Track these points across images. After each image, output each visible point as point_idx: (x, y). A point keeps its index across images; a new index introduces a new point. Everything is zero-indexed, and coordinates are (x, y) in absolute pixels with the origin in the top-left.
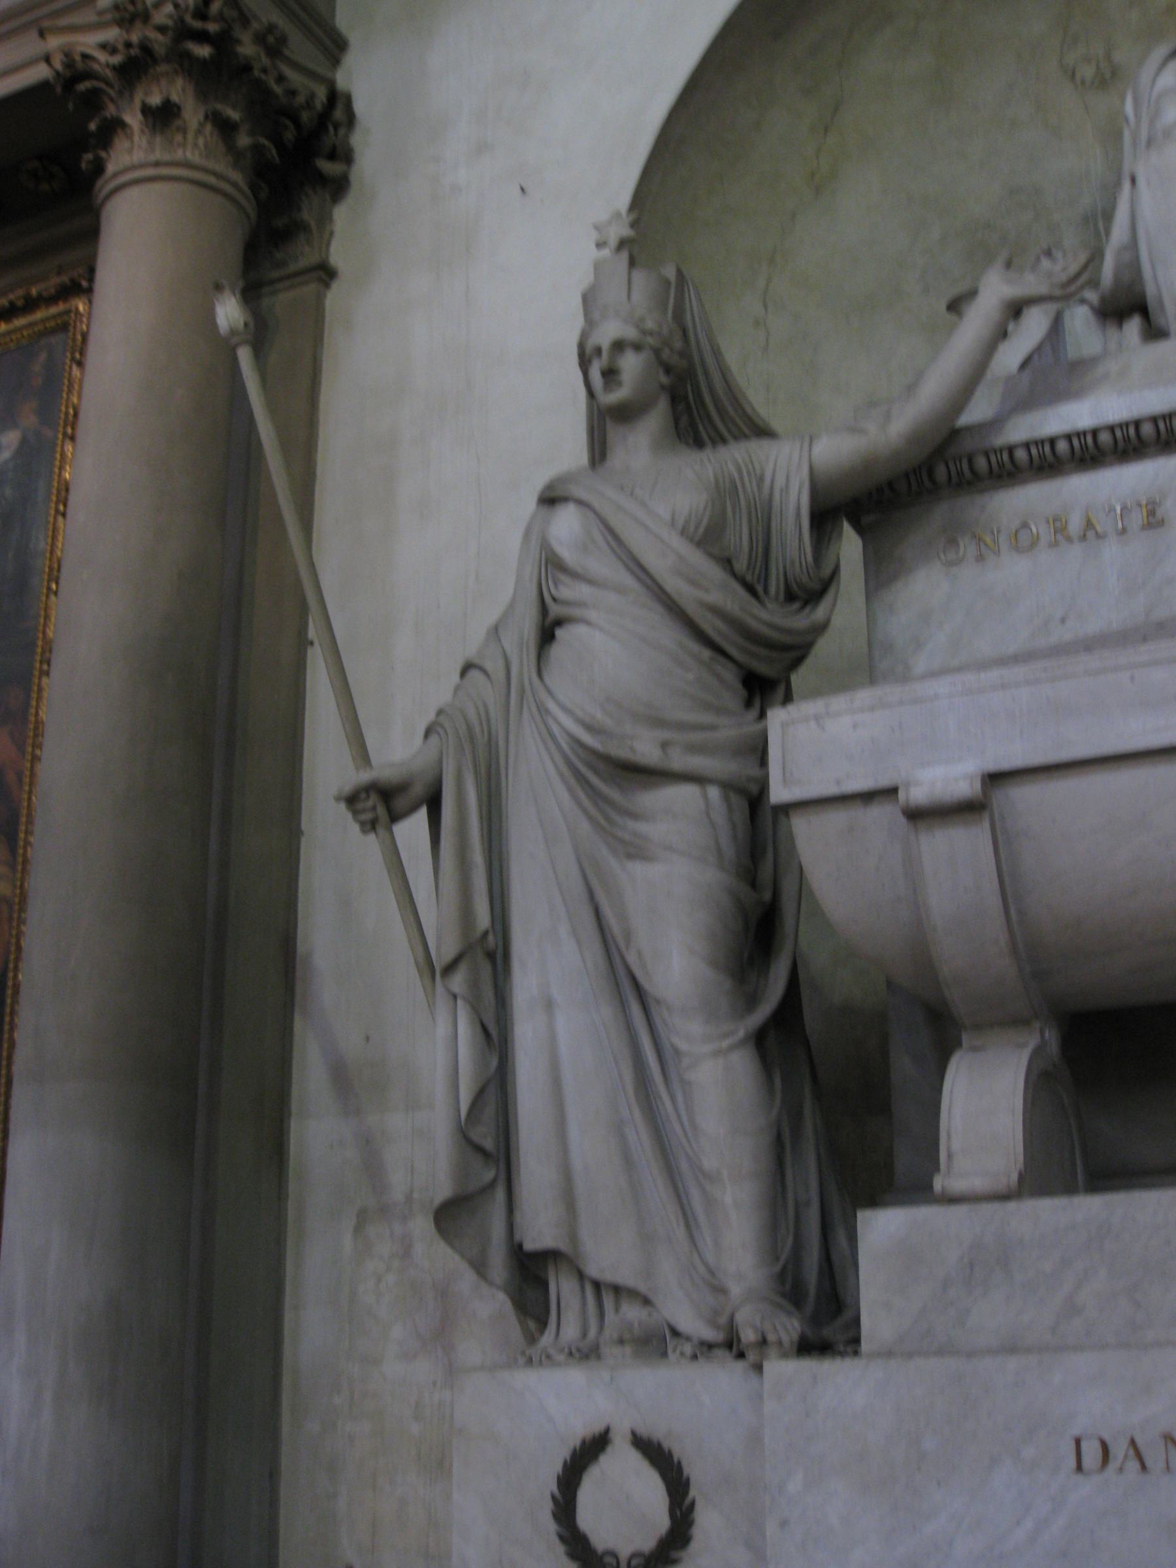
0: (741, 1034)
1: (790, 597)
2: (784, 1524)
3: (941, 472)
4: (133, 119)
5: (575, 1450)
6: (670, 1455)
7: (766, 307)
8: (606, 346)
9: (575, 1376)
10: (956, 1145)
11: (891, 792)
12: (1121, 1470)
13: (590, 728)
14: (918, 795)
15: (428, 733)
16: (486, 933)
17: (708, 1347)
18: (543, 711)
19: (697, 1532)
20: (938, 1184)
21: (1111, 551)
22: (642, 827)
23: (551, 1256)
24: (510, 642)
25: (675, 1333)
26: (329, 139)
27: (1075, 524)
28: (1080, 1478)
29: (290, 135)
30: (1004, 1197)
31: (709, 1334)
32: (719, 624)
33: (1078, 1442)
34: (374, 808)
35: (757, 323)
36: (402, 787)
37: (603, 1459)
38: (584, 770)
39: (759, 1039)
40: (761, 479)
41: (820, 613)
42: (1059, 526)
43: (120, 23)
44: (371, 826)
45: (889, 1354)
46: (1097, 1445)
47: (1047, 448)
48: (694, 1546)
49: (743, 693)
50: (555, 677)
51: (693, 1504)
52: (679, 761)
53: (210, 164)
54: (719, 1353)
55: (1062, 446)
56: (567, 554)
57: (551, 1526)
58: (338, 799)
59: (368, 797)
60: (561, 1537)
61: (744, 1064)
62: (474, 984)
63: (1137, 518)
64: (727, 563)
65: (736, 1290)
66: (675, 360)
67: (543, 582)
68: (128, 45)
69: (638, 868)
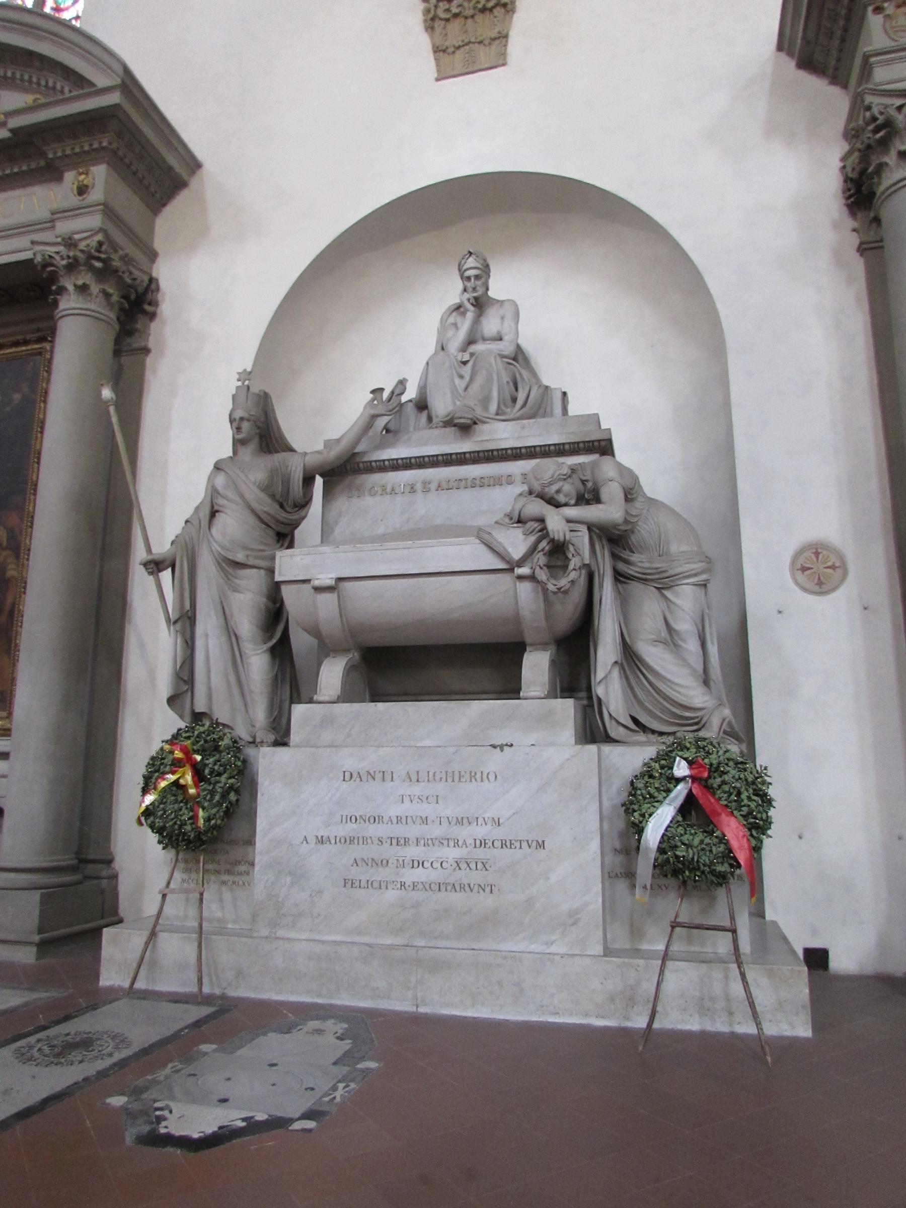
0: (265, 649)
1: (295, 506)
2: (263, 795)
3: (348, 468)
4: (71, 288)
12: (355, 781)
13: (223, 548)
14: (317, 583)
16: (188, 611)
17: (250, 743)
18: (209, 541)
20: (315, 697)
21: (399, 499)
22: (237, 581)
23: (203, 714)
24: (201, 515)
26: (149, 296)
27: (389, 489)
28: (344, 782)
29: (133, 296)
31: (251, 740)
32: (269, 518)
33: (344, 772)
34: (152, 568)
38: (220, 561)
39: (273, 651)
40: (287, 467)
41: (303, 513)
43: (65, 246)
44: (151, 573)
45: (297, 746)
46: (349, 774)
49: (276, 538)
50: (214, 531)
52: (251, 562)
53: (99, 309)
55: (387, 463)
56: (220, 489)
58: (140, 564)
62: (184, 628)
63: (408, 488)
64: (273, 496)
65: (258, 725)
66: (261, 425)
68: (69, 257)
69: (237, 595)
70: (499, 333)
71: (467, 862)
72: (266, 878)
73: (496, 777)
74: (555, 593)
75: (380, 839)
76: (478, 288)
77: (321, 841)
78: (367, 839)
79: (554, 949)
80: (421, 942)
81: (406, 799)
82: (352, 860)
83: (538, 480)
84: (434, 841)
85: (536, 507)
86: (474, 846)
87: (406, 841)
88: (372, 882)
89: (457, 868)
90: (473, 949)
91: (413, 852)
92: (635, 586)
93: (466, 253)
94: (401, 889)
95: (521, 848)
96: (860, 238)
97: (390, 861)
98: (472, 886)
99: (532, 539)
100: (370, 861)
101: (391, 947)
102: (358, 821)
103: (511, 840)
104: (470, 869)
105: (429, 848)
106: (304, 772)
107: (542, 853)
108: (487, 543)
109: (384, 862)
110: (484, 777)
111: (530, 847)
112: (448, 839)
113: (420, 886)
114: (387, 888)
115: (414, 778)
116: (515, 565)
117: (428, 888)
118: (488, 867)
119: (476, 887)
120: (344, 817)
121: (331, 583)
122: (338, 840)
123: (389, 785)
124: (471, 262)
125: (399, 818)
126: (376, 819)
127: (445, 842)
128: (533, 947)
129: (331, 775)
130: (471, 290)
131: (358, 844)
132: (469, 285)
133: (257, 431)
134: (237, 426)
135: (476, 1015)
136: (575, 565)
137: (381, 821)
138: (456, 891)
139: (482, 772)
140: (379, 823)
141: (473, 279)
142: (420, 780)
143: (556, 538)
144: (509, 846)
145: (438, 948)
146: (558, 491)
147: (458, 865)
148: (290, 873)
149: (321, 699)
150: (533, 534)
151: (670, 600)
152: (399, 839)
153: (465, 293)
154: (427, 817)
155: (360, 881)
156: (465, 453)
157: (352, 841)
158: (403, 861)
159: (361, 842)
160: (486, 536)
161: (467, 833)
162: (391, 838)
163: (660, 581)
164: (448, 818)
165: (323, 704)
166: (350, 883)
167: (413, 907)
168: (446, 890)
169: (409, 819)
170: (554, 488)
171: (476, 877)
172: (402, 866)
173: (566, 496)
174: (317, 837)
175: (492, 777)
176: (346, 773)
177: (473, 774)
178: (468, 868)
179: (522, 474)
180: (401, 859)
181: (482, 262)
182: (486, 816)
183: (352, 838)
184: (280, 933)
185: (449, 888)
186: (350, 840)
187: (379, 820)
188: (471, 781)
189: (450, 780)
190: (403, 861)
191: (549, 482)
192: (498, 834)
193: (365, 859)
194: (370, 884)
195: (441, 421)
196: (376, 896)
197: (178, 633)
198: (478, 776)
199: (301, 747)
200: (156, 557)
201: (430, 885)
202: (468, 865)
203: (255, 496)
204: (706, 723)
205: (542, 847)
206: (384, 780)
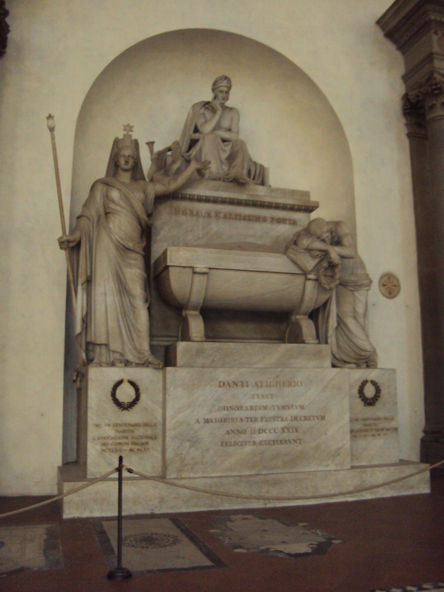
2: (170, 395)
3: (172, 196)
11: (192, 268)
13: (121, 239)
14: (197, 270)
21: (201, 220)
23: (100, 345)
27: (195, 213)
45: (182, 367)
57: (111, 398)
60: (112, 399)
77: (207, 421)
79: (328, 469)
80: (265, 472)
81: (256, 397)
87: (256, 420)
90: (291, 473)
91: (259, 425)
97: (247, 430)
99: (317, 260)
100: (236, 431)
101: (250, 476)
102: (229, 410)
104: (289, 432)
106: (196, 382)
107: (324, 422)
109: (244, 431)
110: (296, 384)
113: (264, 443)
115: (259, 385)
117: (267, 442)
118: (298, 430)
121: (205, 270)
122: (217, 421)
123: (245, 389)
124: (225, 83)
128: (320, 468)
129: (212, 384)
134: (127, 160)
141: (224, 92)
143: (335, 262)
149: (195, 339)
158: (254, 430)
159: (230, 420)
161: (287, 413)
165: (195, 343)
166: (224, 444)
169: (257, 408)
171: (293, 436)
174: (204, 419)
175: (299, 384)
180: (253, 429)
182: (297, 404)
184: (184, 475)
189: (278, 386)
190: (254, 430)
192: (303, 413)
193: (233, 429)
194: (236, 444)
198: (293, 384)
200: (71, 238)
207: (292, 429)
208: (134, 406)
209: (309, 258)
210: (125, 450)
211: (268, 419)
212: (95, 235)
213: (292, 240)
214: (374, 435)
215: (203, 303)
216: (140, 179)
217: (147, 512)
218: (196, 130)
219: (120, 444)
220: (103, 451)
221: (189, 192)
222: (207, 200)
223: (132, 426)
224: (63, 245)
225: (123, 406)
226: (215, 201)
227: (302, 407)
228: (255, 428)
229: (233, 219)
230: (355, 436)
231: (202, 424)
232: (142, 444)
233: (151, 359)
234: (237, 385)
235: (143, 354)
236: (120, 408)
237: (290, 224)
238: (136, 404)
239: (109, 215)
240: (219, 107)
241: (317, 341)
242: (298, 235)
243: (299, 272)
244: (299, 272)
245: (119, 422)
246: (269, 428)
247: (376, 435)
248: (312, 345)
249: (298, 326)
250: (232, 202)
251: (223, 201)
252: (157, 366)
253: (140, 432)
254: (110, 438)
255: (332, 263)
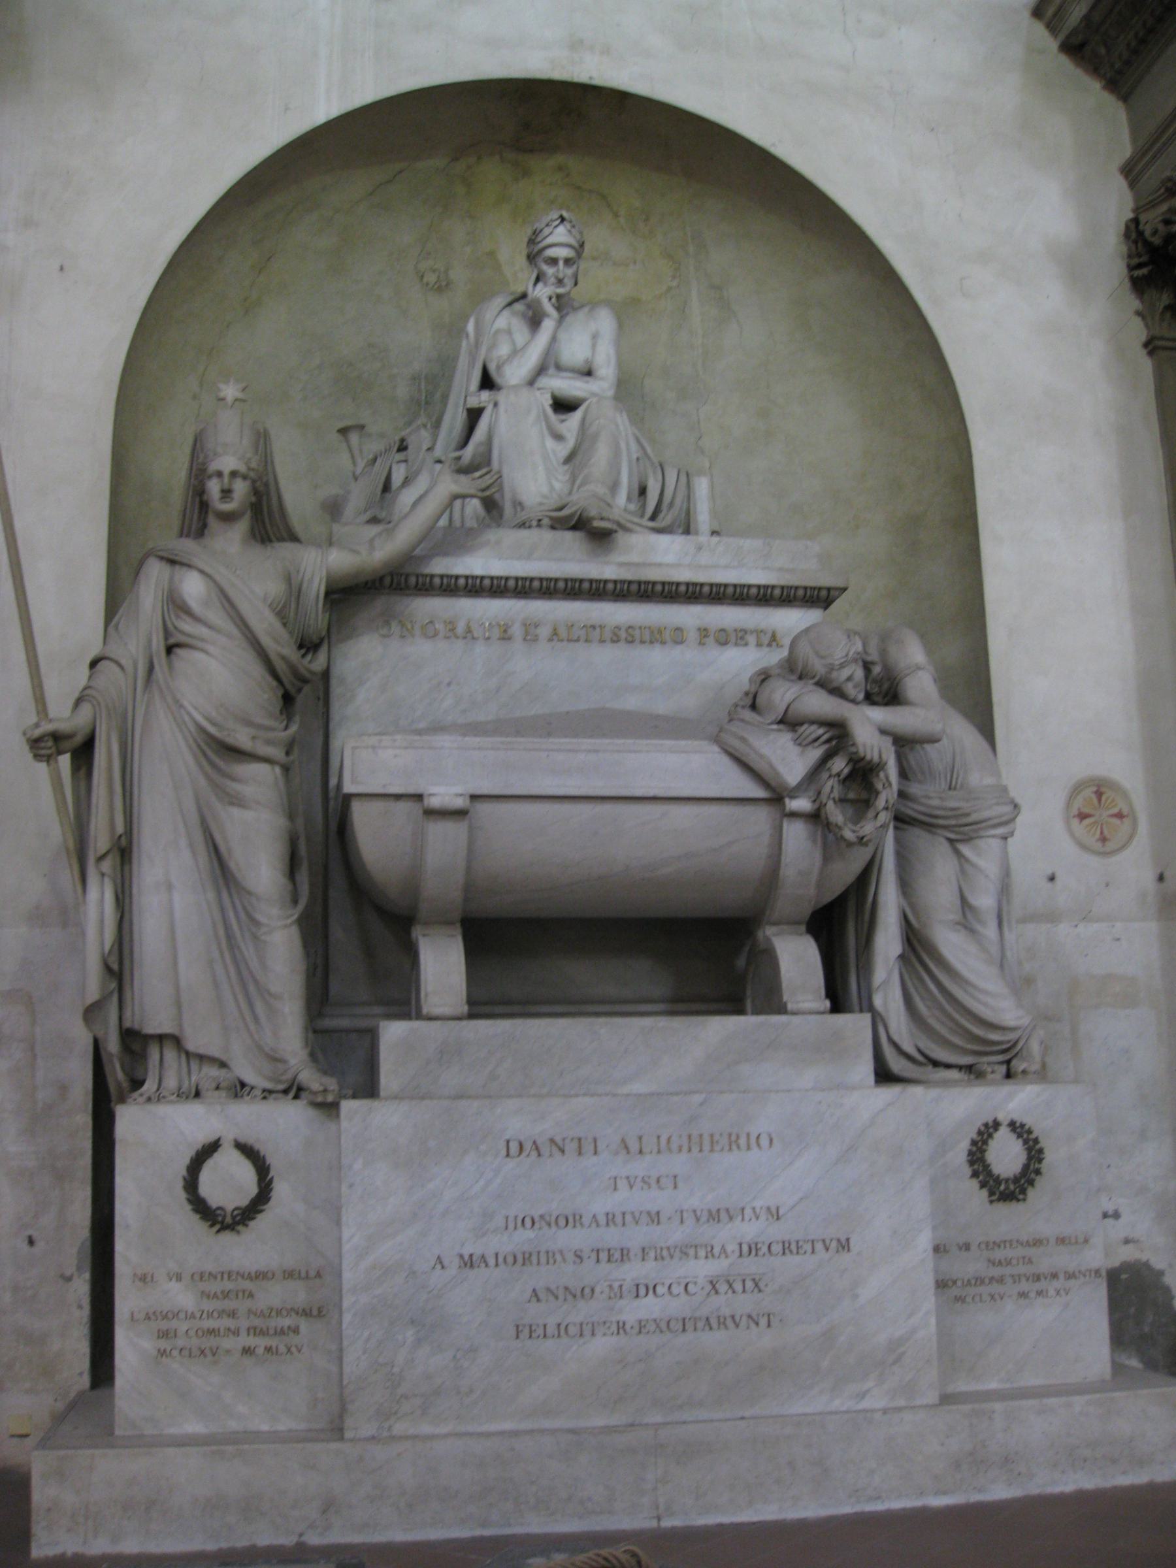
0: (296, 917)
2: (351, 1186)
3: (387, 581)
5: (198, 1151)
6: (258, 1152)
7: (201, 384)
8: (226, 472)
9: (196, 1109)
10: (430, 988)
11: (419, 797)
12: (528, 1155)
14: (435, 802)
15: (78, 702)
19: (274, 1194)
21: (480, 648)
22: (236, 786)
23: (161, 1038)
25: (243, 1085)
27: (461, 628)
28: (508, 1159)
30: (459, 1018)
33: (508, 1142)
34: (50, 748)
35: (195, 397)
36: (69, 736)
37: (216, 1155)
38: (202, 744)
40: (298, 572)
42: (451, 626)
44: (37, 757)
45: (396, 1097)
47: (453, 580)
48: (271, 1203)
51: (272, 1178)
54: (280, 1095)
55: (462, 582)
57: (182, 1195)
59: (47, 741)
61: (294, 931)
63: (496, 633)
65: (293, 1061)
67: (167, 618)
69: (235, 811)
70: (587, 361)
71: (728, 1282)
72: (366, 1334)
73: (771, 1141)
74: (850, 844)
75: (578, 1253)
76: (566, 280)
77: (469, 1262)
78: (554, 1254)
79: (866, 1404)
80: (658, 1419)
82: (529, 1293)
83: (822, 657)
84: (672, 1251)
85: (818, 703)
86: (737, 1253)
87: (624, 1255)
88: (567, 1326)
89: (713, 1292)
90: (743, 1418)
91: (633, 1271)
92: (916, 835)
93: (556, 216)
94: (618, 1333)
95: (813, 1252)
96: (1147, 325)
97: (597, 1290)
98: (737, 1318)
99: (815, 754)
100: (561, 1293)
101: (608, 1430)
102: (537, 1225)
103: (797, 1242)
104: (734, 1292)
105: (666, 1262)
107: (845, 1258)
108: (737, 754)
111: (827, 1249)
112: (696, 1247)
113: (652, 1327)
114: (593, 1334)
115: (634, 1146)
116: (785, 794)
118: (761, 1285)
119: (744, 1319)
120: (511, 1219)
121: (460, 803)
122: (501, 1259)
123: (589, 1160)
125: (610, 1216)
126: (571, 1220)
127: (692, 1252)
128: (837, 1404)
129: (483, 1147)
130: (553, 280)
131: (539, 1263)
132: (550, 271)
133: (253, 499)
134: (226, 487)
135: (755, 1519)
136: (887, 802)
137: (578, 1224)
138: (711, 1328)
139: (748, 1135)
140: (574, 1226)
141: (561, 263)
142: (644, 1150)
143: (868, 757)
144: (795, 1250)
145: (684, 1422)
146: (849, 679)
147: (714, 1287)
148: (413, 1322)
149: (437, 1011)
150: (816, 744)
151: (967, 860)
152: (612, 1252)
153: (540, 285)
154: (658, 1213)
155: (545, 1326)
156: (606, 582)
157: (527, 1259)
158: (621, 1286)
159: (543, 1259)
160: (736, 743)
161: (728, 1234)
162: (598, 1251)
163: (957, 829)
164: (695, 1211)
165: (439, 1023)
166: (526, 1331)
167: (640, 1360)
168: (695, 1329)
169: (628, 1218)
170: (846, 673)
171: (744, 1303)
172: (618, 1294)
173: (855, 687)
174: (461, 1256)
175: (764, 1141)
176: (511, 1144)
177: (733, 1138)
178: (730, 1292)
179: (699, 629)
180: (616, 1285)
181: (578, 237)
182: (758, 1204)
183: (527, 1256)
184: (399, 1428)
185: (700, 1325)
186: (524, 1258)
187: (575, 1221)
188: (730, 1149)
189: (695, 1149)
190: (621, 1286)
191: (841, 664)
192: (777, 1232)
193: (553, 1287)
194: (562, 1330)
195: (547, 516)
196: (575, 1348)
197: (107, 880)
198: (743, 1141)
199: (402, 1099)
200: (63, 727)
201: (668, 1322)
202: (730, 1286)
203: (264, 623)
204: (1021, 1049)
205: (846, 1248)
206: (580, 1154)
207: (744, 1281)
208: (253, 1219)
209: (793, 750)
210: (228, 1351)
211: (665, 1253)
212: (140, 712)
213: (747, 694)
214: (1023, 1295)
215: (466, 900)
216: (281, 539)
217: (288, 1541)
218: (487, 382)
219: (212, 1332)
220: (162, 1353)
221: (440, 566)
222: (497, 588)
223: (250, 1277)
224: (43, 748)
225: (220, 1219)
226: (523, 588)
227: (776, 1215)
228: (624, 1280)
229: (578, 640)
230: (960, 1299)
231: (453, 1270)
232: (281, 1332)
233: (309, 1077)
234: (562, 1151)
235: (283, 1061)
236: (212, 1226)
237: (759, 645)
238: (261, 1211)
239: (178, 651)
240: (548, 307)
241: (828, 1004)
242: (764, 677)
243: (760, 793)
244: (760, 793)
245: (209, 1267)
246: (667, 1283)
247: (1032, 1295)
248: (812, 1018)
249: (769, 957)
250: (574, 590)
251: (547, 589)
252: (320, 1099)
253: (274, 1295)
254: (182, 1315)
255: (863, 759)
